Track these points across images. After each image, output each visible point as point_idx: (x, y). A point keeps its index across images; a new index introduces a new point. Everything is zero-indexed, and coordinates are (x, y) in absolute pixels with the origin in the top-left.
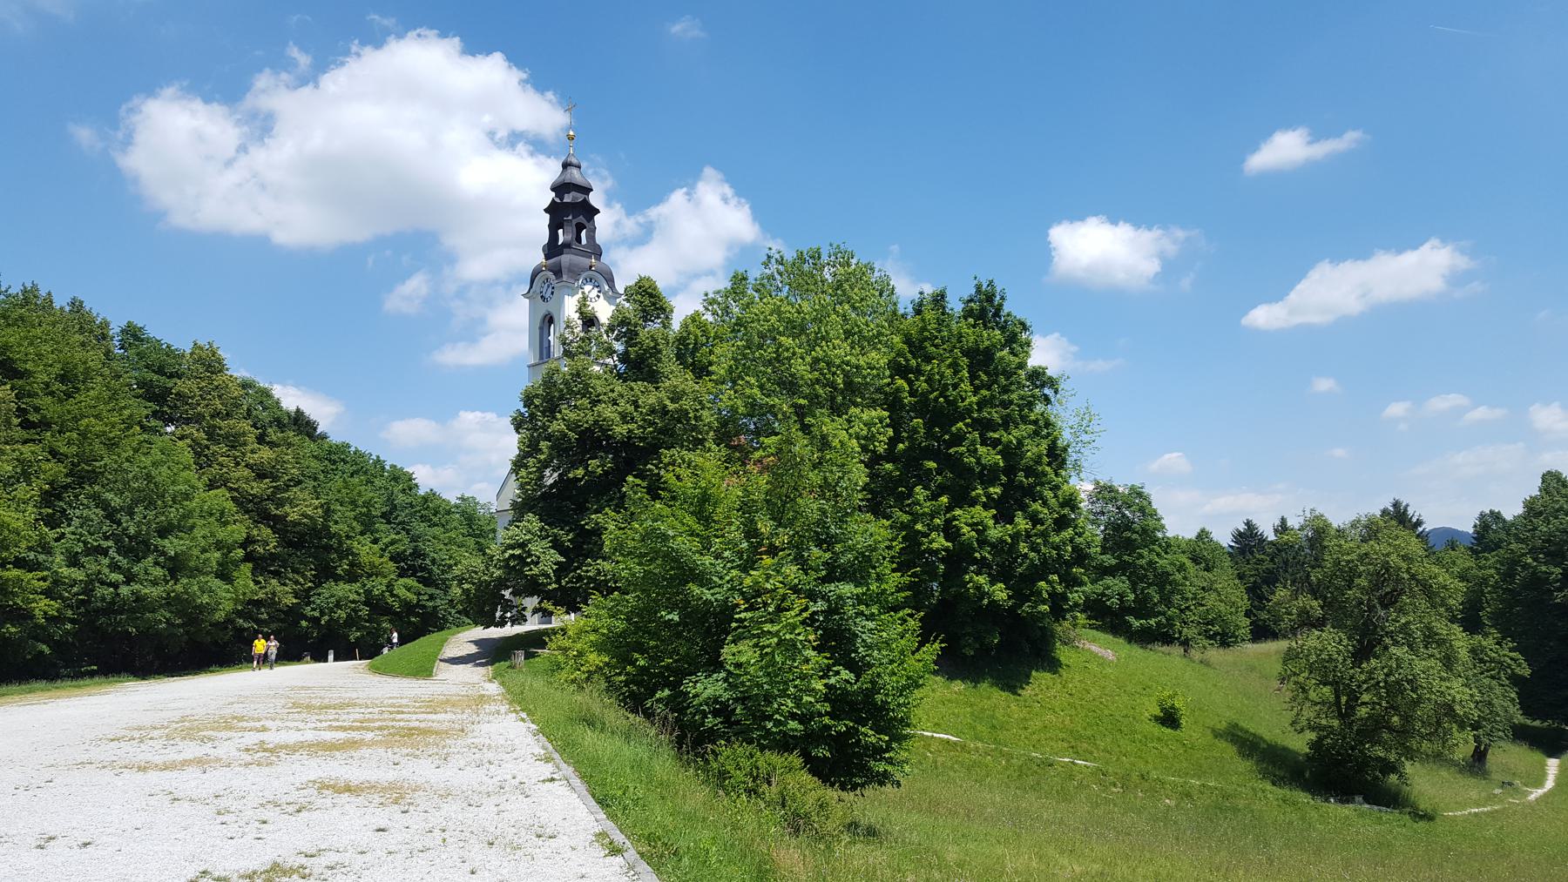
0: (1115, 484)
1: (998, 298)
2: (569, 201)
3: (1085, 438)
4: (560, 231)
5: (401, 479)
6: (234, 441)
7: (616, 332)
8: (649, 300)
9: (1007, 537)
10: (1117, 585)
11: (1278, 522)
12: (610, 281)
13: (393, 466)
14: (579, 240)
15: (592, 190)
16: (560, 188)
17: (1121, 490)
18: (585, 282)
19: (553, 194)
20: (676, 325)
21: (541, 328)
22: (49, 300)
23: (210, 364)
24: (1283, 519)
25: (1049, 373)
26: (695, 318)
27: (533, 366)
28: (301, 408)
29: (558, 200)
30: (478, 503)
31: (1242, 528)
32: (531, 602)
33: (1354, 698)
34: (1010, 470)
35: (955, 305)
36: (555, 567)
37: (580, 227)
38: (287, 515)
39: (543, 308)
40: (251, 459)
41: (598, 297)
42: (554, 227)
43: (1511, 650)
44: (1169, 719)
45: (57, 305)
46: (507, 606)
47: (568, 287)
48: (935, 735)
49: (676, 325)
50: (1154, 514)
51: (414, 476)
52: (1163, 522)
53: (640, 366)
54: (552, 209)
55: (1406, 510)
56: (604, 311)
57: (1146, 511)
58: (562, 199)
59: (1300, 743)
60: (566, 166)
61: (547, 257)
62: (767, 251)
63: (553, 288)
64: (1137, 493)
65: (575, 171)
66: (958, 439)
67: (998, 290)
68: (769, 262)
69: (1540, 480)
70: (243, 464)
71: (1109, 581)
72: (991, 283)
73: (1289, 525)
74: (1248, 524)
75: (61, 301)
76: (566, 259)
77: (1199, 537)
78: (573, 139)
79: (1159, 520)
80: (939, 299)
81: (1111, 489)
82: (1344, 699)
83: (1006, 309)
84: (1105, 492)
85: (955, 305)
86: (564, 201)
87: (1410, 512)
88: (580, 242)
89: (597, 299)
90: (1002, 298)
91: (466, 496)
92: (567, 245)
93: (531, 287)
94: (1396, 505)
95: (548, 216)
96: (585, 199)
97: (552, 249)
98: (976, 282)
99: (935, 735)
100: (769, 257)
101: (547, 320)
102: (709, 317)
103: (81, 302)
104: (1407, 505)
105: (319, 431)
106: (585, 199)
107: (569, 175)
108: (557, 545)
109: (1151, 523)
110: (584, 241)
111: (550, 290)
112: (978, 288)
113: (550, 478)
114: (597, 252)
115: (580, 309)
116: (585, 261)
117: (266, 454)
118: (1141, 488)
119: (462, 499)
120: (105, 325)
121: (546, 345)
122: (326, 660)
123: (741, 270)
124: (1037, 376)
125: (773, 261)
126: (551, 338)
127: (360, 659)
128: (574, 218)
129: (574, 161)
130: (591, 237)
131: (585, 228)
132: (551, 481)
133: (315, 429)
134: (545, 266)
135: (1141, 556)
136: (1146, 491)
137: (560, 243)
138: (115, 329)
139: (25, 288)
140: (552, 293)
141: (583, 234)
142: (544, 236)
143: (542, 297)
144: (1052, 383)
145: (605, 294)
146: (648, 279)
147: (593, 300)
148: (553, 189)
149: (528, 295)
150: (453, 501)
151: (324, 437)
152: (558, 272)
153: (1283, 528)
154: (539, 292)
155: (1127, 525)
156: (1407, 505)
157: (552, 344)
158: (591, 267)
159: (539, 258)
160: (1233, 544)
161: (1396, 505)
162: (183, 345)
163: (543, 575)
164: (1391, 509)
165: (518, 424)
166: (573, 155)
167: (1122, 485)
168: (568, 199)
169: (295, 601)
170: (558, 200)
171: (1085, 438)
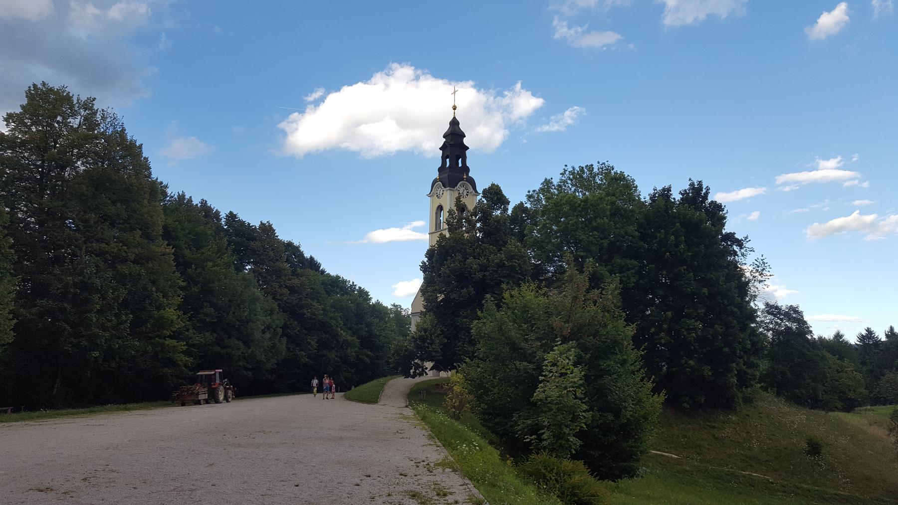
0: (779, 305)
1: (704, 191)
2: (452, 143)
6: (278, 273)
7: (477, 217)
9: (710, 336)
13: (360, 288)
14: (458, 164)
17: (783, 308)
18: (460, 187)
19: (444, 140)
20: (510, 212)
21: (436, 213)
22: (190, 200)
25: (736, 236)
26: (520, 208)
28: (313, 256)
30: (402, 309)
32: (429, 365)
35: (676, 196)
36: (441, 347)
38: (305, 314)
41: (467, 195)
42: (444, 158)
45: (195, 203)
46: (417, 366)
48: (664, 454)
50: (805, 322)
51: (369, 294)
52: (811, 329)
57: (801, 322)
64: (794, 309)
65: (456, 127)
67: (704, 187)
68: (565, 171)
70: (284, 286)
72: (700, 183)
75: (196, 201)
78: (456, 109)
80: (666, 192)
81: (777, 308)
83: (710, 200)
84: (772, 309)
85: (676, 196)
91: (396, 304)
93: (431, 191)
99: (664, 454)
100: (565, 171)
101: (439, 209)
102: (528, 205)
103: (206, 201)
105: (321, 268)
110: (460, 165)
112: (692, 185)
113: (441, 297)
114: (466, 169)
115: (457, 203)
117: (296, 282)
118: (797, 308)
119: (394, 305)
120: (218, 213)
121: (438, 222)
123: (549, 178)
124: (730, 237)
125: (567, 173)
126: (441, 218)
127: (340, 392)
130: (464, 162)
132: (441, 298)
133: (320, 267)
136: (800, 309)
138: (223, 215)
139: (179, 195)
140: (443, 194)
143: (437, 196)
144: (740, 243)
146: (498, 186)
147: (464, 197)
148: (444, 137)
150: (390, 307)
151: (323, 272)
157: (442, 222)
159: (436, 175)
162: (256, 223)
163: (435, 352)
165: (424, 268)
169: (307, 360)
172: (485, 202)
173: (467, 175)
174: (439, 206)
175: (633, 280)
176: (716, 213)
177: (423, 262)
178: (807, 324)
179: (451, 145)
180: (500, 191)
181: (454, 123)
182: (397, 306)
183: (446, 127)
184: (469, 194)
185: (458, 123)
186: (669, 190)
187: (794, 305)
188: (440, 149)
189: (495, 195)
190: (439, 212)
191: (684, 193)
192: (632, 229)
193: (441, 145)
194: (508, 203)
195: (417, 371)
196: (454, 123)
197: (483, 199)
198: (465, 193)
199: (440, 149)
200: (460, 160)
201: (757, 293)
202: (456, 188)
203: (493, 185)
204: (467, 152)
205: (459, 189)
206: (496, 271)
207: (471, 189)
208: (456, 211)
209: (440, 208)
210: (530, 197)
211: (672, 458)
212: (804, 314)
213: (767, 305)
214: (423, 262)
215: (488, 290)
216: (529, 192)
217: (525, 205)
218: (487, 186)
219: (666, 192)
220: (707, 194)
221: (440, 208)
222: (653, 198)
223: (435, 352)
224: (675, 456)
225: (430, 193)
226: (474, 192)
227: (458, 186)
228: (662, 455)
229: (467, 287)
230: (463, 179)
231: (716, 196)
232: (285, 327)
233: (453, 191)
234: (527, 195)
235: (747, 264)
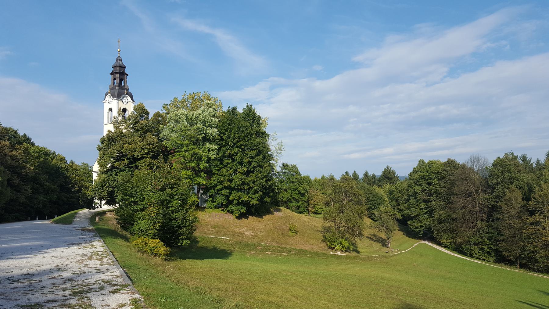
0: (289, 164)
2: (118, 72)
3: (279, 152)
4: (115, 81)
8: (142, 111)
11: (353, 172)
18: (123, 98)
19: (113, 69)
20: (151, 116)
24: (355, 172)
26: (158, 114)
29: (114, 72)
31: (345, 174)
32: (103, 202)
34: (250, 163)
35: (240, 110)
37: (121, 80)
41: (128, 103)
48: (222, 238)
49: (151, 116)
54: (112, 73)
56: (130, 108)
57: (297, 173)
60: (117, 60)
61: (111, 89)
62: (185, 92)
64: (294, 167)
65: (120, 62)
69: (418, 162)
73: (356, 173)
74: (347, 173)
77: (322, 178)
78: (120, 51)
79: (300, 175)
80: (234, 109)
84: (285, 166)
85: (240, 110)
87: (392, 169)
88: (122, 85)
89: (127, 103)
91: (85, 163)
94: (388, 167)
95: (111, 76)
98: (247, 105)
104: (391, 168)
107: (118, 63)
109: (297, 176)
110: (123, 85)
111: (111, 100)
112: (248, 106)
113: (109, 165)
115: (119, 112)
119: (83, 163)
124: (264, 133)
131: (123, 80)
134: (110, 93)
136: (297, 166)
137: (115, 84)
140: (112, 101)
141: (123, 82)
147: (126, 104)
148: (113, 67)
149: (104, 102)
150: (80, 164)
153: (355, 176)
156: (391, 168)
161: (388, 167)
164: (387, 169)
165: (100, 149)
166: (120, 56)
171: (279, 152)
172: (136, 113)
173: (127, 90)
174: (110, 108)
175: (215, 156)
177: (98, 145)
178: (300, 173)
179: (117, 73)
180: (144, 107)
181: (119, 59)
182: (85, 164)
183: (113, 62)
184: (129, 102)
185: (121, 60)
187: (295, 164)
188: (110, 74)
191: (244, 109)
193: (110, 73)
194: (148, 113)
195: (96, 206)
196: (119, 59)
197: (134, 112)
198: (127, 102)
199: (110, 74)
200: (123, 81)
201: (278, 159)
205: (122, 99)
206: (140, 152)
208: (118, 117)
209: (111, 110)
210: (164, 108)
211: (226, 239)
212: (298, 168)
213: (283, 164)
214: (98, 145)
215: (136, 162)
216: (164, 104)
217: (161, 112)
218: (136, 104)
219: (234, 109)
220: (255, 109)
221: (111, 110)
222: (228, 111)
223: (105, 195)
224: (228, 238)
226: (132, 101)
228: (221, 238)
229: (124, 160)
230: (125, 94)
231: (258, 112)
233: (119, 100)
234: (163, 106)
235: (272, 145)
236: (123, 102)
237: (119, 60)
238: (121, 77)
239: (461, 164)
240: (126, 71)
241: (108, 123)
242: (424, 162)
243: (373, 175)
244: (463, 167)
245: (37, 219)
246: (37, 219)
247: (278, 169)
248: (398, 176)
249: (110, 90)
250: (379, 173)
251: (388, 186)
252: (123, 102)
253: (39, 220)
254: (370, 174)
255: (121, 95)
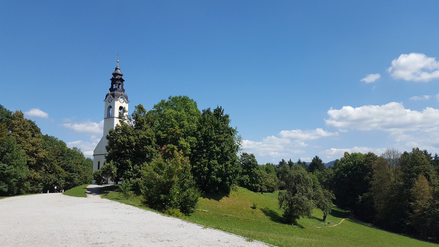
0: (247, 153)
1: (222, 110)
4: (114, 85)
5: (62, 144)
10: (246, 177)
11: (289, 160)
12: (127, 98)
14: (119, 87)
15: (123, 75)
16: (115, 74)
17: (249, 154)
21: (108, 109)
23: (20, 116)
26: (150, 112)
27: (106, 118)
29: (114, 77)
31: (281, 161)
33: (292, 204)
35: (212, 111)
37: (119, 84)
39: (109, 104)
40: (31, 141)
42: (112, 84)
43: (332, 193)
44: (254, 208)
46: (104, 180)
47: (116, 100)
53: (139, 125)
55: (318, 158)
57: (254, 161)
58: (115, 77)
59: (281, 213)
60: (116, 69)
63: (112, 99)
64: (252, 156)
66: (211, 145)
71: (245, 176)
72: (221, 107)
74: (283, 160)
76: (115, 92)
81: (246, 154)
82: (290, 203)
84: (245, 155)
86: (116, 78)
87: (319, 158)
90: (223, 111)
92: (116, 89)
93: (106, 99)
94: (316, 157)
95: (111, 81)
96: (121, 78)
97: (112, 89)
104: (319, 157)
106: (121, 78)
108: (117, 166)
110: (120, 88)
111: (111, 100)
112: (218, 107)
114: (124, 91)
116: (121, 93)
117: (34, 140)
121: (109, 114)
122: (47, 193)
128: (118, 81)
129: (119, 68)
130: (122, 87)
134: (110, 94)
135: (252, 170)
141: (120, 86)
142: (110, 87)
143: (109, 101)
145: (125, 101)
148: (112, 74)
149: (105, 101)
152: (113, 95)
154: (108, 100)
155: (250, 163)
156: (319, 157)
157: (111, 113)
158: (122, 95)
160: (279, 165)
161: (316, 157)
164: (315, 158)
167: (249, 153)
168: (117, 77)
170: (114, 77)
174: (110, 106)
176: (225, 119)
183: (113, 71)
186: (210, 109)
187: (252, 153)
188: (111, 80)
189: (140, 108)
190: (109, 110)
192: (195, 125)
199: (111, 80)
200: (121, 85)
202: (118, 99)
203: (140, 104)
204: (124, 82)
207: (126, 100)
213: (243, 154)
225: (105, 100)
226: (127, 101)
227: (119, 98)
232: (28, 162)
236: (120, 101)
237: (118, 69)
238: (120, 82)
239: (379, 156)
240: (123, 78)
241: (107, 117)
242: (349, 155)
243: (304, 163)
244: (381, 158)
245: (48, 192)
246: (48, 192)
247: (240, 157)
248: (324, 163)
249: (110, 92)
250: (309, 160)
251: (317, 172)
252: (120, 101)
253: (49, 192)
254: (302, 161)
255: (119, 97)
